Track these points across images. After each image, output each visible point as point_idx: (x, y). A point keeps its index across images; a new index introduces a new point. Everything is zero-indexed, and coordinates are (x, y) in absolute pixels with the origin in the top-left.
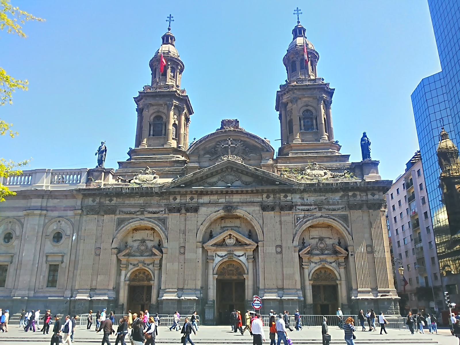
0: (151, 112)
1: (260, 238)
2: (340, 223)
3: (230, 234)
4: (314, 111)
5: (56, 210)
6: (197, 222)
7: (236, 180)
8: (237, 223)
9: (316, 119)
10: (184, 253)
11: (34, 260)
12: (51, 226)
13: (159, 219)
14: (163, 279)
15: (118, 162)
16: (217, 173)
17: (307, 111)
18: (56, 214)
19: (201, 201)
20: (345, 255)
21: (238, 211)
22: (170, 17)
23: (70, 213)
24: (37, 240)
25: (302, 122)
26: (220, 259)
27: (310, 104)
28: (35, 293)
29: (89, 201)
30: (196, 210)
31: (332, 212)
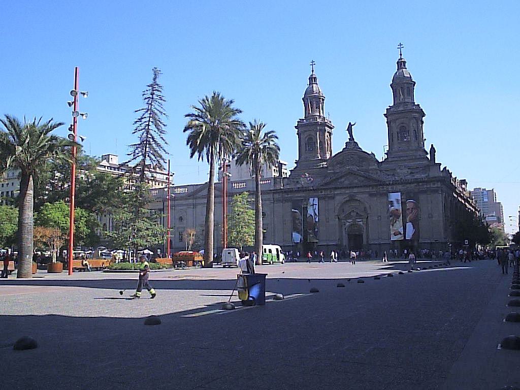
0: (306, 135)
1: (369, 212)
4: (407, 127)
8: (357, 204)
10: (329, 222)
16: (343, 176)
19: (336, 193)
25: (399, 135)
26: (348, 223)
27: (405, 122)
29: (277, 196)
30: (333, 198)
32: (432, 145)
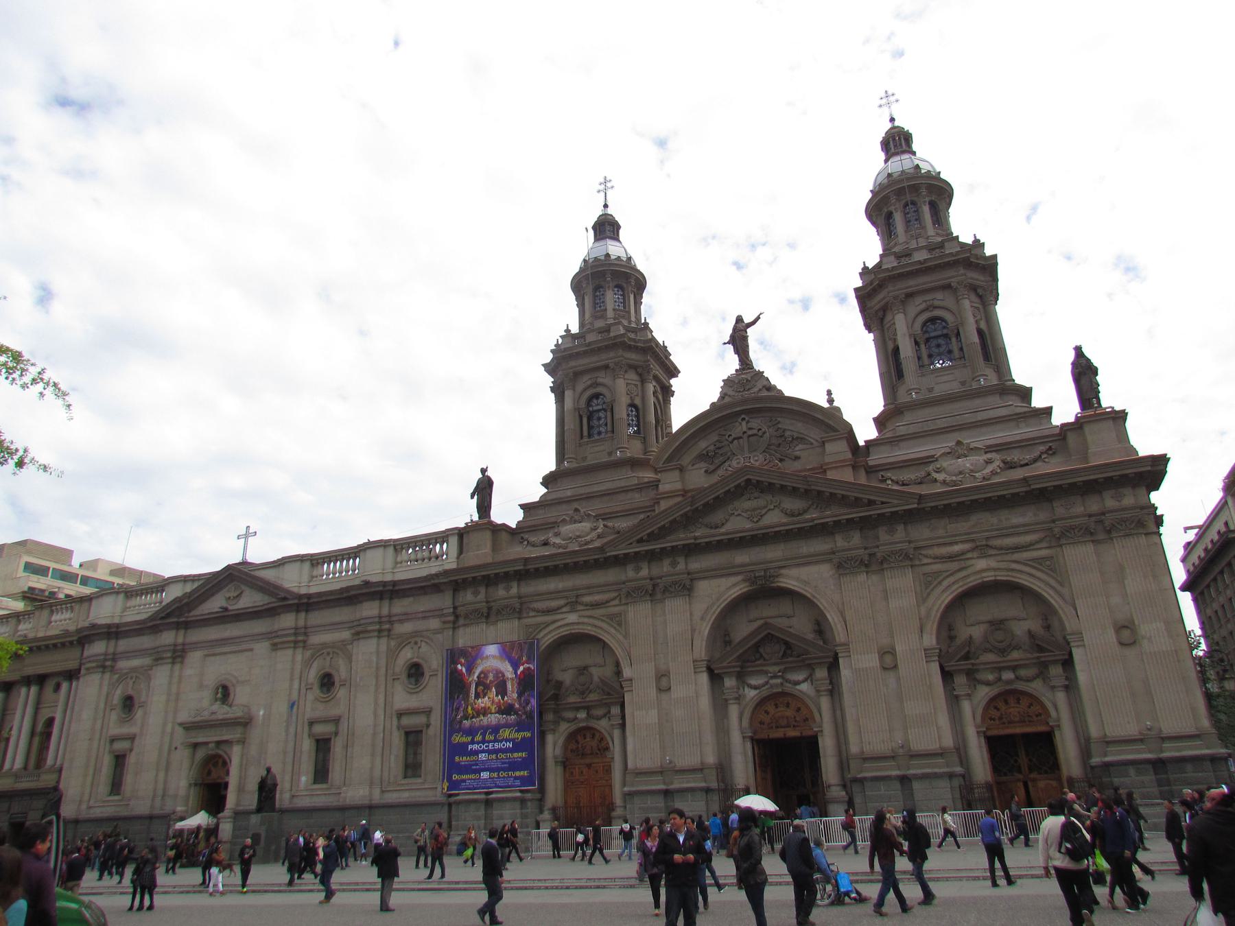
0: (580, 387)
1: (840, 635)
2: (1039, 579)
3: (769, 633)
5: (408, 620)
6: (691, 614)
7: (770, 510)
8: (785, 607)
9: (958, 334)
11: (375, 726)
12: (403, 653)
13: (611, 617)
14: (630, 748)
15: (520, 505)
17: (933, 320)
18: (407, 627)
20: (1061, 657)
21: (781, 580)
22: (606, 181)
23: (434, 624)
24: (377, 686)
27: (936, 303)
28: (383, 792)
29: (468, 597)
30: (685, 588)
31: (1013, 553)
32: (1078, 351)
